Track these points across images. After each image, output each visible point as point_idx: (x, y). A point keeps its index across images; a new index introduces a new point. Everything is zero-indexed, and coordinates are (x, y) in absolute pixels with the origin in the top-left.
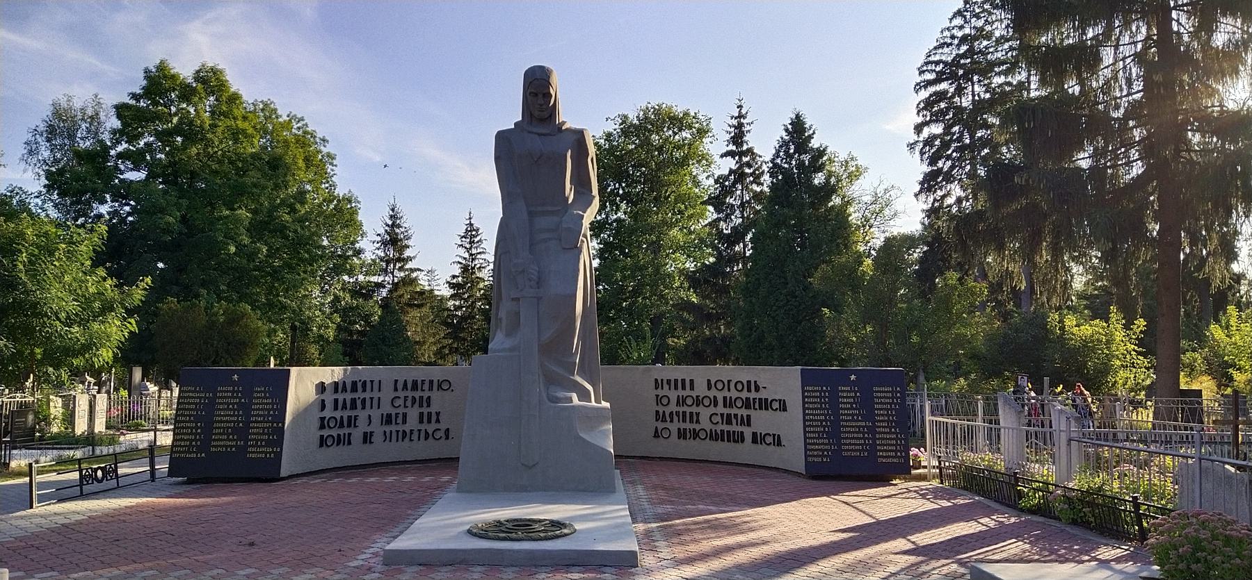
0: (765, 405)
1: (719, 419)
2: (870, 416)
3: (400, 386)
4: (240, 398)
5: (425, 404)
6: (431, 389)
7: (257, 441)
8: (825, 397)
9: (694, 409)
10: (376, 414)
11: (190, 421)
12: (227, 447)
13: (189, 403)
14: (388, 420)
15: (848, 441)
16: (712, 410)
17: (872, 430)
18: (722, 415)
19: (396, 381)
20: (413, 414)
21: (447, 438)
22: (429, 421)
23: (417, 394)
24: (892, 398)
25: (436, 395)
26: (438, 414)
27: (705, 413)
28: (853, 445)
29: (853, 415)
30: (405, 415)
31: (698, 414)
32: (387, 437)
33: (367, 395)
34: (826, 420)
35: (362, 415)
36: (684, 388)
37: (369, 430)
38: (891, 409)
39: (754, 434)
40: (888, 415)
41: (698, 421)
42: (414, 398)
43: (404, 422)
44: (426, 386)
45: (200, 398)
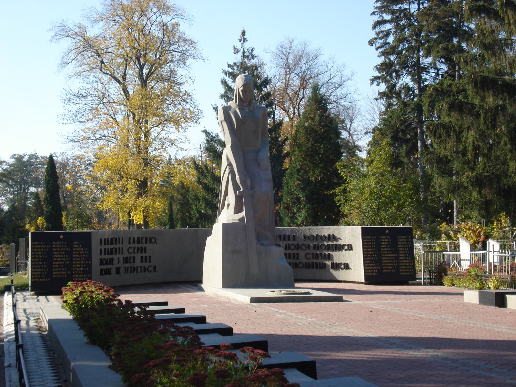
0: (340, 248)
1: (310, 256)
2: (396, 251)
3: (132, 241)
4: (66, 248)
5: (144, 251)
6: (146, 243)
7: (78, 271)
8: (373, 242)
9: (296, 251)
10: (121, 257)
11: (39, 261)
12: (62, 274)
13: (38, 251)
14: (126, 260)
15: (385, 265)
16: (307, 251)
17: (397, 258)
18: (313, 254)
19: (130, 238)
25: (149, 246)
26: (150, 257)
27: (302, 253)
28: (388, 266)
29: (387, 251)
30: (134, 258)
31: (298, 254)
32: (126, 270)
33: (118, 246)
35: (115, 257)
36: (289, 239)
37: (118, 266)
38: (406, 247)
39: (332, 264)
40: (405, 250)
41: (298, 258)
42: (138, 248)
43: (134, 262)
44: (144, 241)
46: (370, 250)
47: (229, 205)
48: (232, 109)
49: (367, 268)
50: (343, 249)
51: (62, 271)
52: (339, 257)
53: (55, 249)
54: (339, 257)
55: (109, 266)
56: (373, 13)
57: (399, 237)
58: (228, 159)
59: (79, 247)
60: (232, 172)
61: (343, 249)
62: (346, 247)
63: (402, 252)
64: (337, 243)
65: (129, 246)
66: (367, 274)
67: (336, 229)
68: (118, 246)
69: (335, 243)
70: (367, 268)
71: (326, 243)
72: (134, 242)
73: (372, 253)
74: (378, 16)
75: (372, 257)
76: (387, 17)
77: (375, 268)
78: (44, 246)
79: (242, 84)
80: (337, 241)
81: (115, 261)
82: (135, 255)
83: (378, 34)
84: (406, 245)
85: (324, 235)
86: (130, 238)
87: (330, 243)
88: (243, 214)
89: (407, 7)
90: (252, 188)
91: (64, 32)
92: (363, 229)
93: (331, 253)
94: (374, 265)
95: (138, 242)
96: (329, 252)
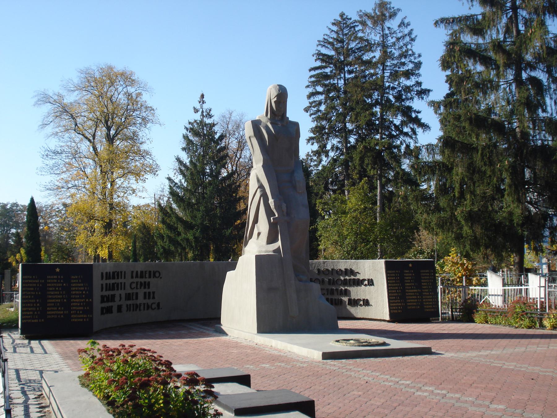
0: (359, 283)
4: (63, 283)
6: (150, 277)
7: (77, 310)
8: (397, 277)
10: (123, 292)
11: (31, 299)
12: (58, 315)
14: (128, 297)
18: (327, 289)
19: (132, 272)
20: (141, 292)
21: (159, 308)
22: (149, 298)
23: (143, 280)
24: (429, 276)
25: (152, 281)
26: (154, 293)
30: (137, 294)
32: (129, 308)
33: (120, 281)
34: (398, 289)
35: (117, 293)
37: (120, 303)
39: (350, 300)
43: (137, 298)
44: (147, 275)
45: (36, 283)
46: (395, 285)
47: (259, 234)
48: (262, 124)
49: (391, 305)
50: (362, 284)
51: (58, 310)
52: (357, 292)
53: (50, 285)
54: (357, 292)
55: (110, 304)
56: (308, 86)
57: (422, 271)
58: (258, 180)
59: (79, 283)
60: (264, 195)
61: (362, 284)
62: (366, 282)
63: (425, 287)
64: (356, 278)
65: (132, 280)
66: (392, 311)
67: (354, 263)
68: (120, 281)
69: (352, 277)
70: (391, 305)
71: (342, 278)
72: (137, 277)
73: (397, 288)
74: (312, 89)
75: (397, 292)
76: (320, 89)
77: (399, 304)
78: (38, 281)
79: (276, 94)
80: (356, 276)
81: (117, 298)
82: (138, 291)
83: (311, 103)
84: (429, 279)
85: (340, 270)
86: (132, 272)
87: (347, 278)
88: (279, 243)
89: (336, 82)
90: (288, 214)
91: (45, 99)
92: (386, 263)
93: (348, 288)
94: (399, 301)
95: (142, 277)
96: (346, 288)
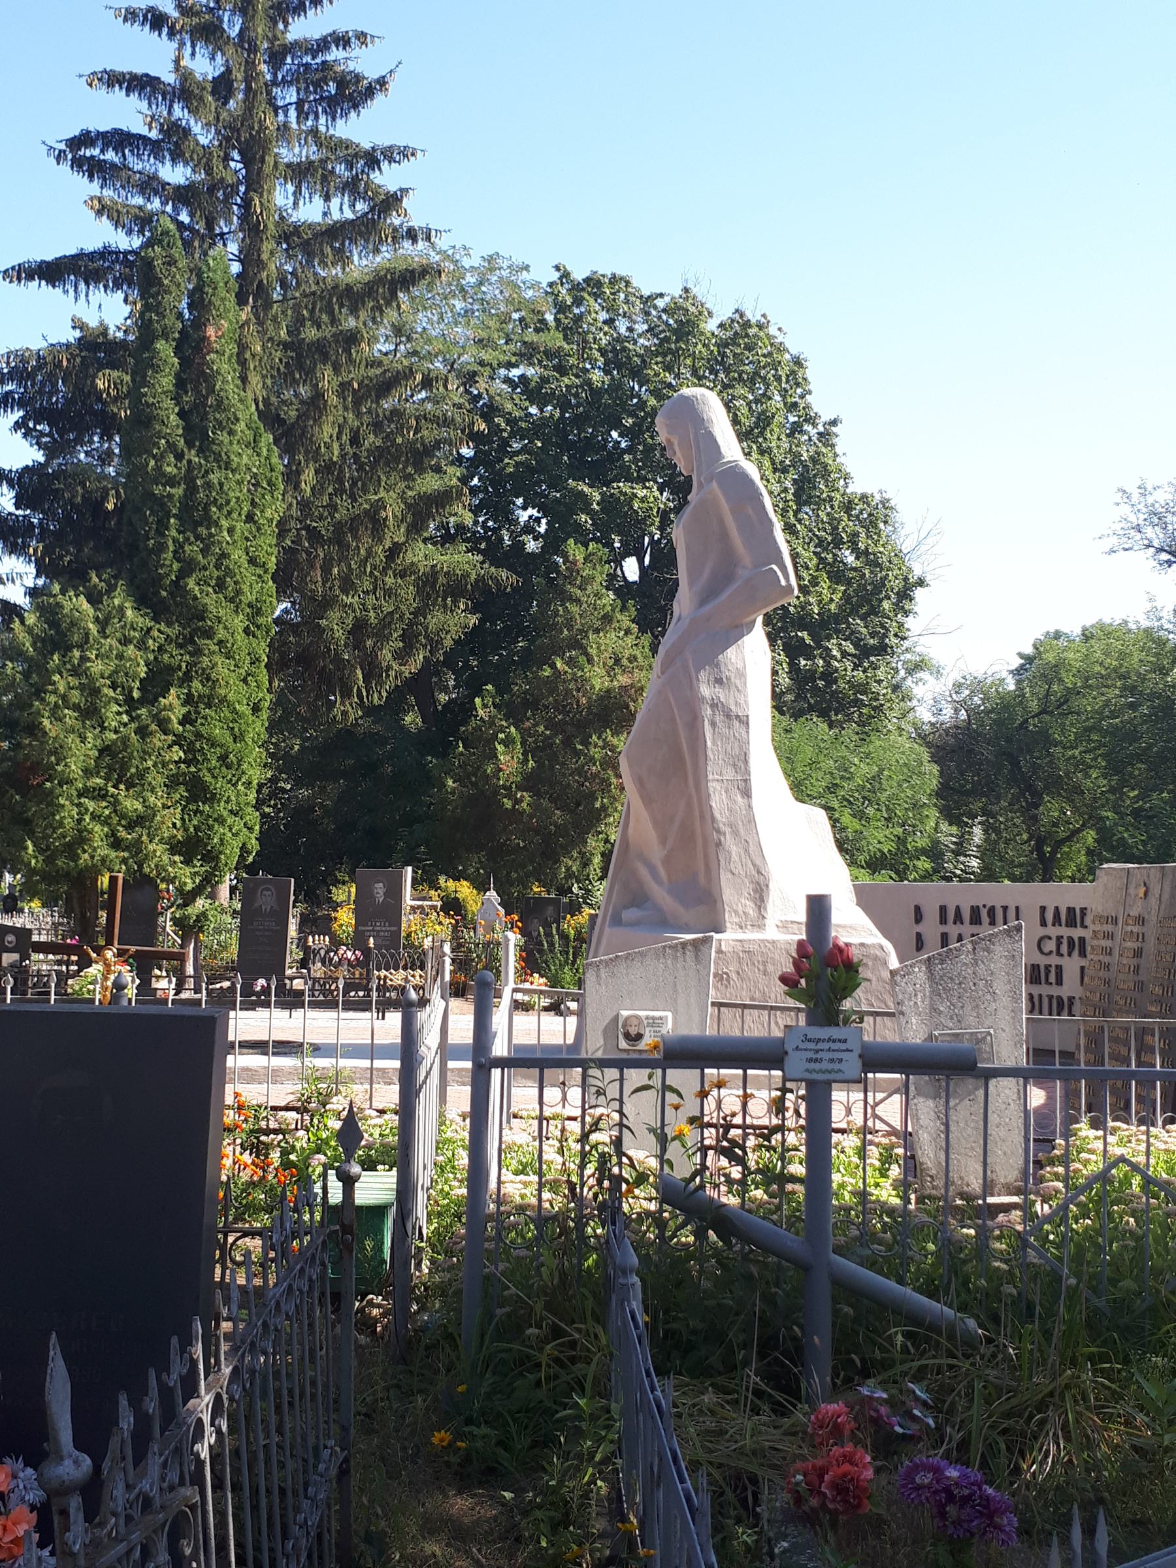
19: (1043, 909)
30: (1059, 969)
43: (1059, 982)
65: (1042, 931)
72: (1057, 920)
82: (1065, 962)
86: (1043, 909)
95: (1071, 923)
